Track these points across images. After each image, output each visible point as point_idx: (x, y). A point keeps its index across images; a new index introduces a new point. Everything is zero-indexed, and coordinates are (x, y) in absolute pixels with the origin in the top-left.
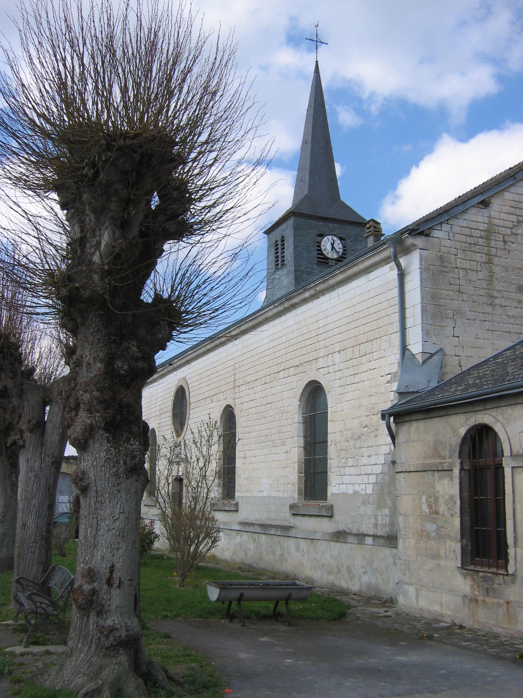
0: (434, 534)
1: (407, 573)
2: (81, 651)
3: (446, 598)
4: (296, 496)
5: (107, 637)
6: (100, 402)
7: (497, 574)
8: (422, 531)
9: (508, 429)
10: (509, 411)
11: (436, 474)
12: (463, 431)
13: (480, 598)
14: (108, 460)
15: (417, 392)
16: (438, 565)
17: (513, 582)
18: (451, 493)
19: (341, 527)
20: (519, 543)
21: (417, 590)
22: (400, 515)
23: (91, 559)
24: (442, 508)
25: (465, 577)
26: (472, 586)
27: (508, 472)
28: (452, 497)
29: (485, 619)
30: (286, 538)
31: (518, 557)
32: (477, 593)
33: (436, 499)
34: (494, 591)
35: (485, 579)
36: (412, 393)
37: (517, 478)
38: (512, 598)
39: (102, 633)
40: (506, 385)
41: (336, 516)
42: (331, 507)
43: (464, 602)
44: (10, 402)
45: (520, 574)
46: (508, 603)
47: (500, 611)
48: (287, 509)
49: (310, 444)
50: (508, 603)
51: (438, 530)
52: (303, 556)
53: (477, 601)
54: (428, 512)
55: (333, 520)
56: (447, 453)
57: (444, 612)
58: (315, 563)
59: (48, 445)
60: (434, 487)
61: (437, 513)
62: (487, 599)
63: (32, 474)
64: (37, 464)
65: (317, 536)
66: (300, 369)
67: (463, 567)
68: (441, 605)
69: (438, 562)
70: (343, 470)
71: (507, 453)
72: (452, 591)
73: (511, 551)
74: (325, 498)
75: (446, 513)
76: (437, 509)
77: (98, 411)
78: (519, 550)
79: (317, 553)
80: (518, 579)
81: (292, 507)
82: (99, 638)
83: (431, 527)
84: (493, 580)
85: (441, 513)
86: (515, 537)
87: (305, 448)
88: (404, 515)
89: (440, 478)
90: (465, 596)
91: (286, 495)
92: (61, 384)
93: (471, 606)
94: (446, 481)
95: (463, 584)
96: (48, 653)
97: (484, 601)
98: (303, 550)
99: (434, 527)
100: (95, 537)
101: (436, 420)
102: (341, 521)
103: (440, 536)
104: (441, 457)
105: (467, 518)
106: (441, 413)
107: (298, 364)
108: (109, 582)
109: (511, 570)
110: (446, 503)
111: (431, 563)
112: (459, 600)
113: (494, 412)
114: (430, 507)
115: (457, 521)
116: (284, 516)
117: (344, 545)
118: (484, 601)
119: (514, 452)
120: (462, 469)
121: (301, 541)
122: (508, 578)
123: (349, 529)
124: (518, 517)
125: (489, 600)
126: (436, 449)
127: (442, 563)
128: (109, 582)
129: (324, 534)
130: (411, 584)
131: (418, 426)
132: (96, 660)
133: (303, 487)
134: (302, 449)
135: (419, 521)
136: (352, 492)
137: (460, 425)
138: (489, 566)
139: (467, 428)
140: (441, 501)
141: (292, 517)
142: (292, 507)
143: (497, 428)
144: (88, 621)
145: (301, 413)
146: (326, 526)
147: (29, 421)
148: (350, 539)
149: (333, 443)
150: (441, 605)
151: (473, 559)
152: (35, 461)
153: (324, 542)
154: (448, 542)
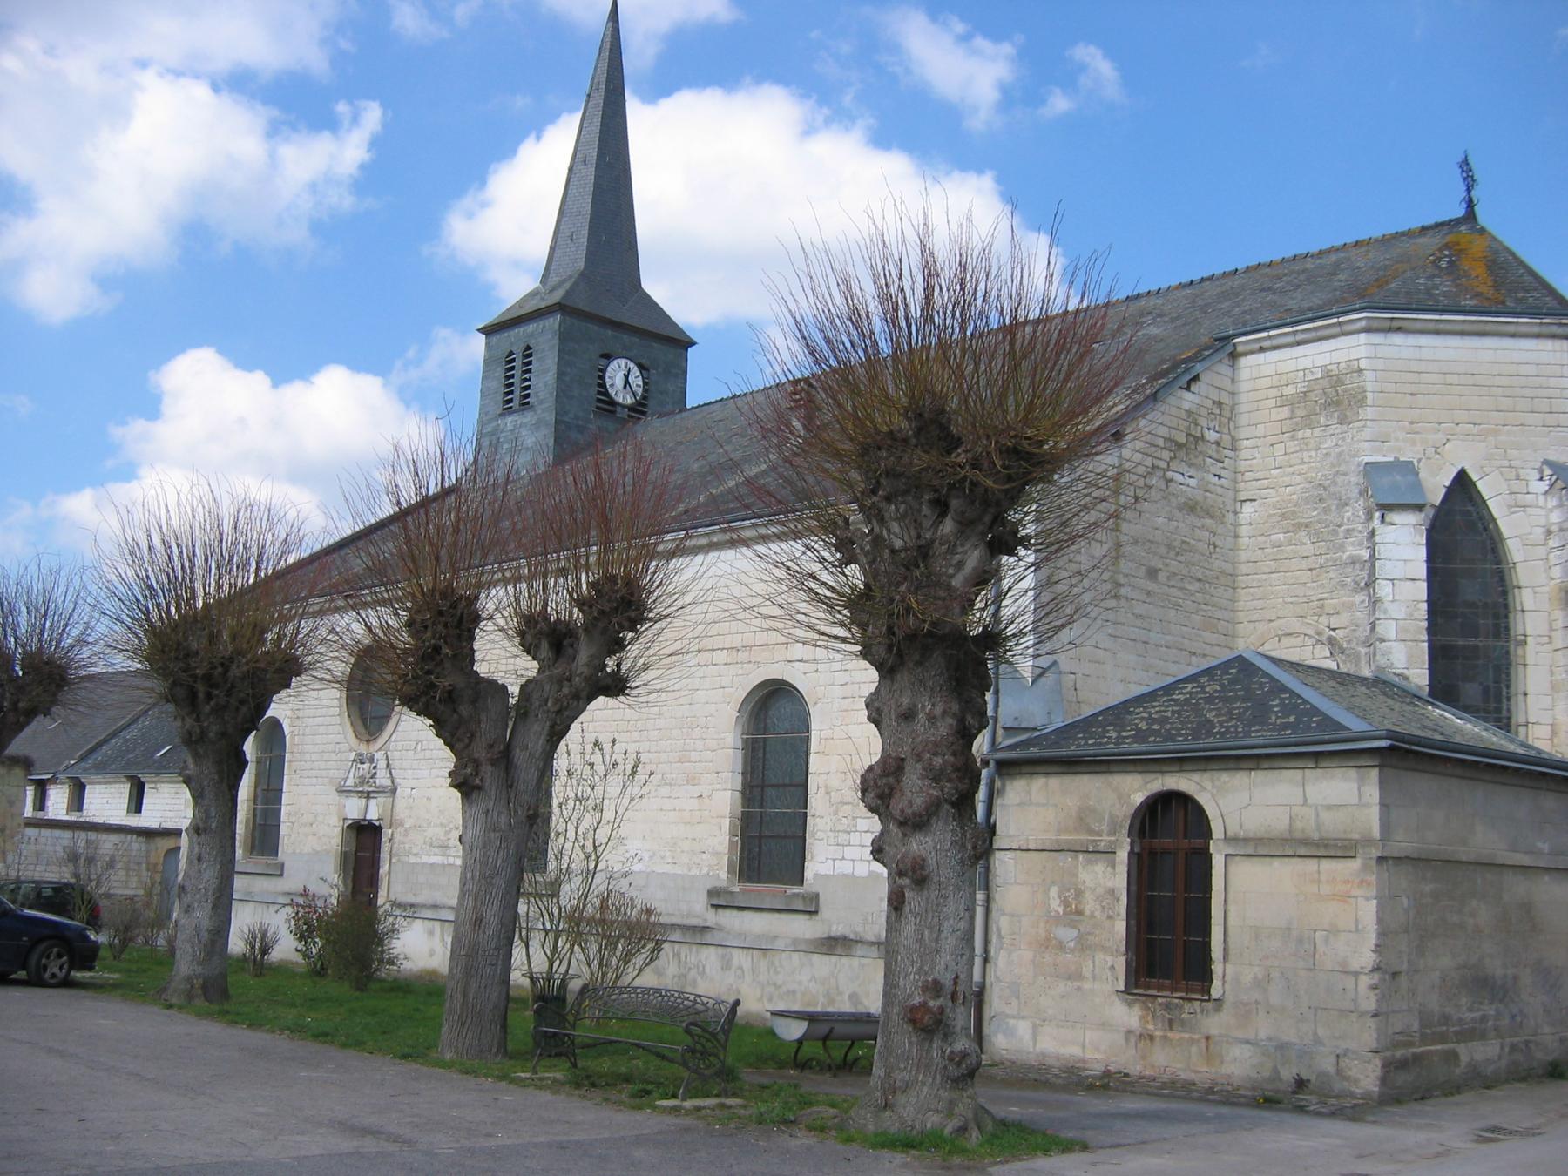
0: (1072, 944)
1: (1015, 1002)
2: (924, 1084)
3: (1091, 1036)
4: (723, 875)
5: (959, 1064)
6: (957, 769)
7: (1190, 1000)
8: (1048, 939)
9: (1221, 802)
10: (1225, 777)
11: (1081, 857)
12: (1138, 798)
13: (1158, 1033)
14: (954, 843)
15: (1035, 729)
16: (1079, 989)
17: (1218, 1009)
18: (1110, 884)
19: (837, 930)
20: (1231, 957)
21: (1035, 1027)
22: (1004, 914)
23: (932, 968)
24: (1090, 905)
25: (1130, 1004)
26: (1141, 1018)
27: (1218, 862)
28: (1112, 892)
29: (1171, 1059)
30: (694, 947)
31: (1228, 978)
32: (1151, 1027)
33: (1079, 894)
34: (1183, 1022)
35: (1167, 1007)
36: (1026, 730)
37: (1232, 868)
38: (1214, 1032)
39: (951, 1060)
40: (1231, 742)
41: (826, 912)
42: (815, 897)
43: (1127, 1040)
44: (455, 711)
45: (1229, 999)
46: (1208, 1038)
47: (1194, 1049)
48: (703, 897)
49: (752, 787)
50: (1208, 1038)
51: (1080, 939)
52: (742, 977)
53: (1152, 1038)
54: (1061, 910)
55: (818, 918)
56: (1104, 827)
57: (1089, 1055)
58: (772, 989)
59: (521, 787)
60: (1076, 876)
61: (1079, 913)
62: (1169, 1034)
63: (494, 836)
64: (503, 819)
65: (779, 944)
66: (742, 656)
67: (1127, 991)
68: (1084, 1047)
69: (1076, 984)
70: (846, 836)
71: (1217, 832)
72: (1104, 1025)
73: (1217, 968)
74: (800, 880)
75: (1097, 914)
76: (1081, 907)
77: (949, 781)
78: (1230, 969)
79: (776, 973)
80: (1227, 1005)
81: (713, 893)
82: (945, 1068)
83: (1067, 934)
84: (1182, 1007)
85: (1087, 912)
86: (1225, 950)
87: (743, 793)
88: (1012, 915)
89: (1089, 862)
90: (1129, 1032)
91: (695, 872)
92: (547, 688)
93: (1141, 1045)
94: (1100, 868)
95: (1128, 1016)
96: (723, 1106)
97: (1165, 1037)
98: (741, 968)
99: (1075, 933)
100: (937, 940)
101: (1086, 778)
102: (834, 920)
103: (1084, 946)
104: (1090, 831)
105: (1133, 922)
106: (1103, 768)
107: (739, 645)
108: (954, 998)
109: (1215, 994)
110: (1099, 899)
111: (1062, 987)
112: (1119, 1039)
113: (1196, 777)
114: (1066, 903)
115: (1121, 927)
116: (697, 909)
117: (844, 960)
118: (1165, 1037)
119: (1230, 833)
120: (1131, 853)
121: (735, 952)
122: (1209, 1005)
123: (856, 933)
124: (1231, 922)
125: (1174, 1035)
126: (1083, 819)
127: (1087, 986)
128: (954, 998)
129: (796, 941)
130: (1023, 1018)
131: (1046, 785)
132: (944, 1095)
133: (736, 859)
134: (738, 795)
135: (1042, 925)
136: (865, 874)
137: (1136, 789)
138: (1174, 989)
139: (1147, 794)
140: (1089, 896)
141: (712, 912)
142: (713, 893)
143: (1203, 799)
144: (930, 1046)
145: (739, 731)
146: (801, 927)
147: (491, 746)
148: (860, 950)
149: (822, 791)
150: (1084, 1047)
151: (1137, 980)
152: (500, 813)
153: (796, 956)
154: (1100, 956)
